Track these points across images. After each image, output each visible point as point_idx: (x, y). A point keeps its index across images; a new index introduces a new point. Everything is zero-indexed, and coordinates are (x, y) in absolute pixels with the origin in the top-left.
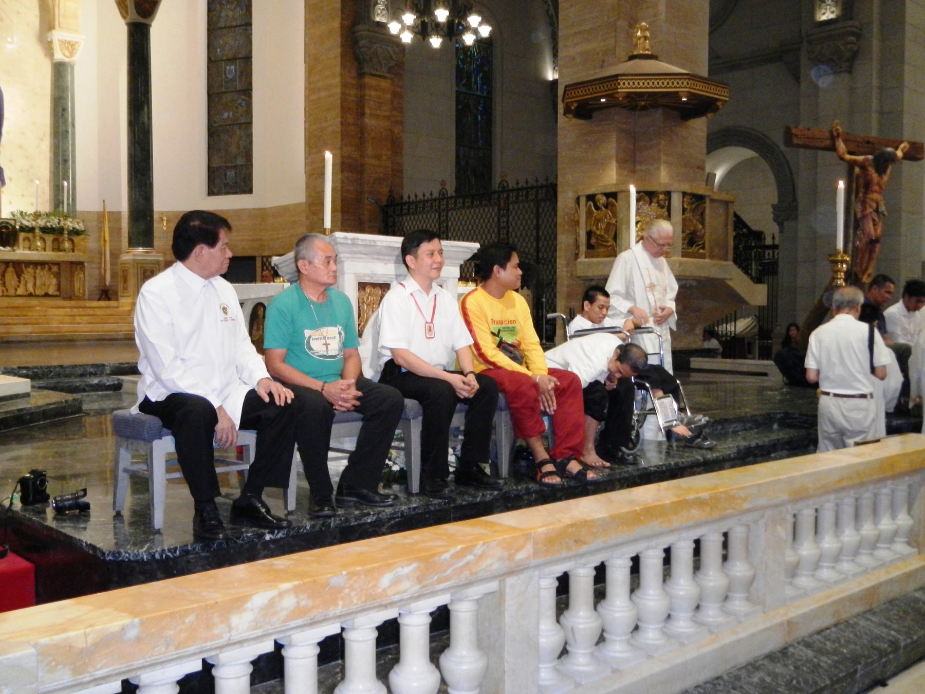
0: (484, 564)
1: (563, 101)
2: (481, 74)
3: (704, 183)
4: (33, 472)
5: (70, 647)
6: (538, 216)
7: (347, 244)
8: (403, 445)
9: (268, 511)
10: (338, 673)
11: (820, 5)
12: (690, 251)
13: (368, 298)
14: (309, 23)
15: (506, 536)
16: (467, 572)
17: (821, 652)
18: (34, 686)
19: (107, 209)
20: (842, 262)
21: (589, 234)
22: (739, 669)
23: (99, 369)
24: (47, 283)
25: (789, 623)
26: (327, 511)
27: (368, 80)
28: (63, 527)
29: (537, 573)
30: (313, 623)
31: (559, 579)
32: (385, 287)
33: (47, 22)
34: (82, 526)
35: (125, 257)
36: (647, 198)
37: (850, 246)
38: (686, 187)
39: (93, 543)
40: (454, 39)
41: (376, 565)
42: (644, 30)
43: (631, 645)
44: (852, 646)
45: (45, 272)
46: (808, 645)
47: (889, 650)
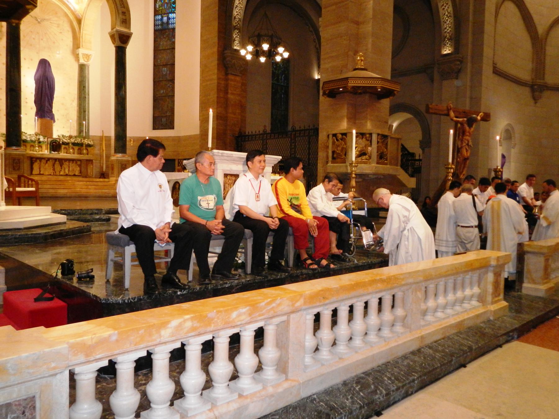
0: (280, 308)
1: (322, 89)
2: (283, 76)
4: (67, 260)
5: (84, 344)
6: (309, 143)
7: (219, 155)
8: (243, 251)
9: (179, 281)
10: (210, 357)
13: (228, 181)
14: (203, 49)
15: (291, 295)
16: (272, 312)
17: (437, 351)
18: (67, 362)
19: (105, 135)
20: (451, 168)
21: (333, 152)
22: (398, 358)
23: (99, 211)
24: (75, 169)
25: (422, 337)
26: (207, 281)
27: (231, 77)
28: (81, 287)
29: (305, 312)
30: (199, 335)
31: (315, 315)
32: (237, 176)
33: (76, 45)
34: (91, 286)
35: (113, 158)
36: (361, 136)
37: (455, 161)
39: (97, 295)
40: (271, 58)
41: (230, 308)
42: (361, 56)
43: (348, 346)
44: (451, 348)
45: (74, 164)
46: (430, 348)
47: (468, 350)
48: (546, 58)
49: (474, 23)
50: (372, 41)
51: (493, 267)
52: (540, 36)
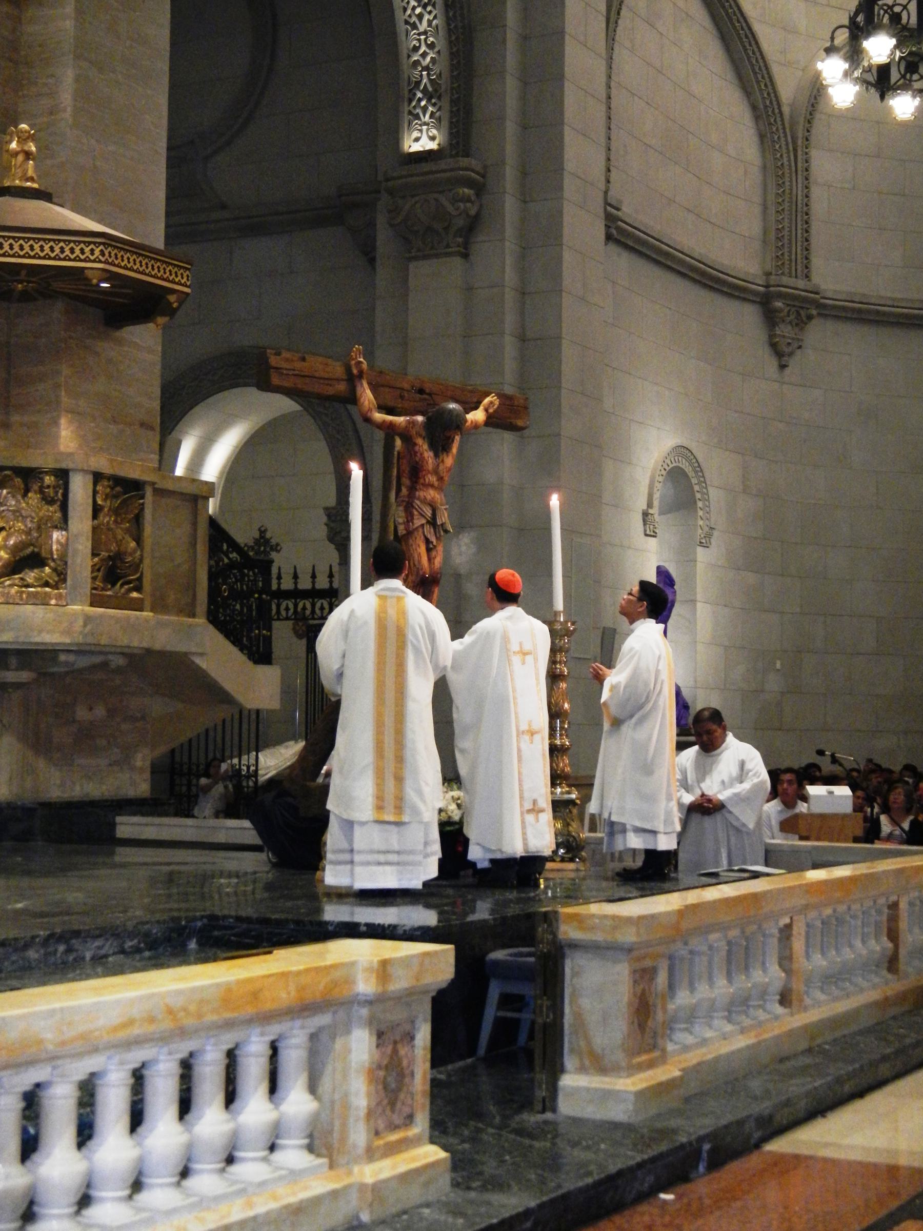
3: (157, 457)
11: (410, 123)
12: (109, 593)
36: (18, 481)
38: (102, 463)
48: (816, 193)
49: (525, 38)
50: (77, 79)
51: (370, 1002)
52: (786, 110)
